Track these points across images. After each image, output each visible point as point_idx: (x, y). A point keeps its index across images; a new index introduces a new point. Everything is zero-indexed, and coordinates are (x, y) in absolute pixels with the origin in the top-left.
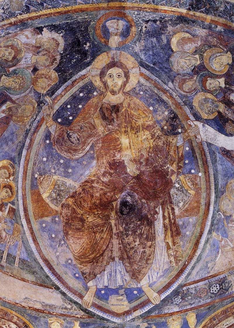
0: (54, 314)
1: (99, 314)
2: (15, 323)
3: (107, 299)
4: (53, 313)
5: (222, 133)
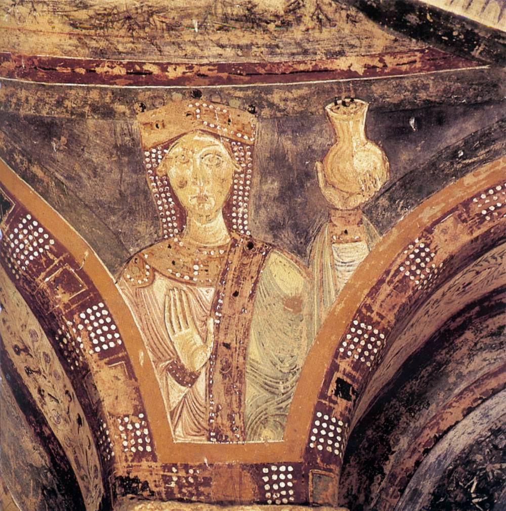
0: (172, 74)
4: (164, 67)
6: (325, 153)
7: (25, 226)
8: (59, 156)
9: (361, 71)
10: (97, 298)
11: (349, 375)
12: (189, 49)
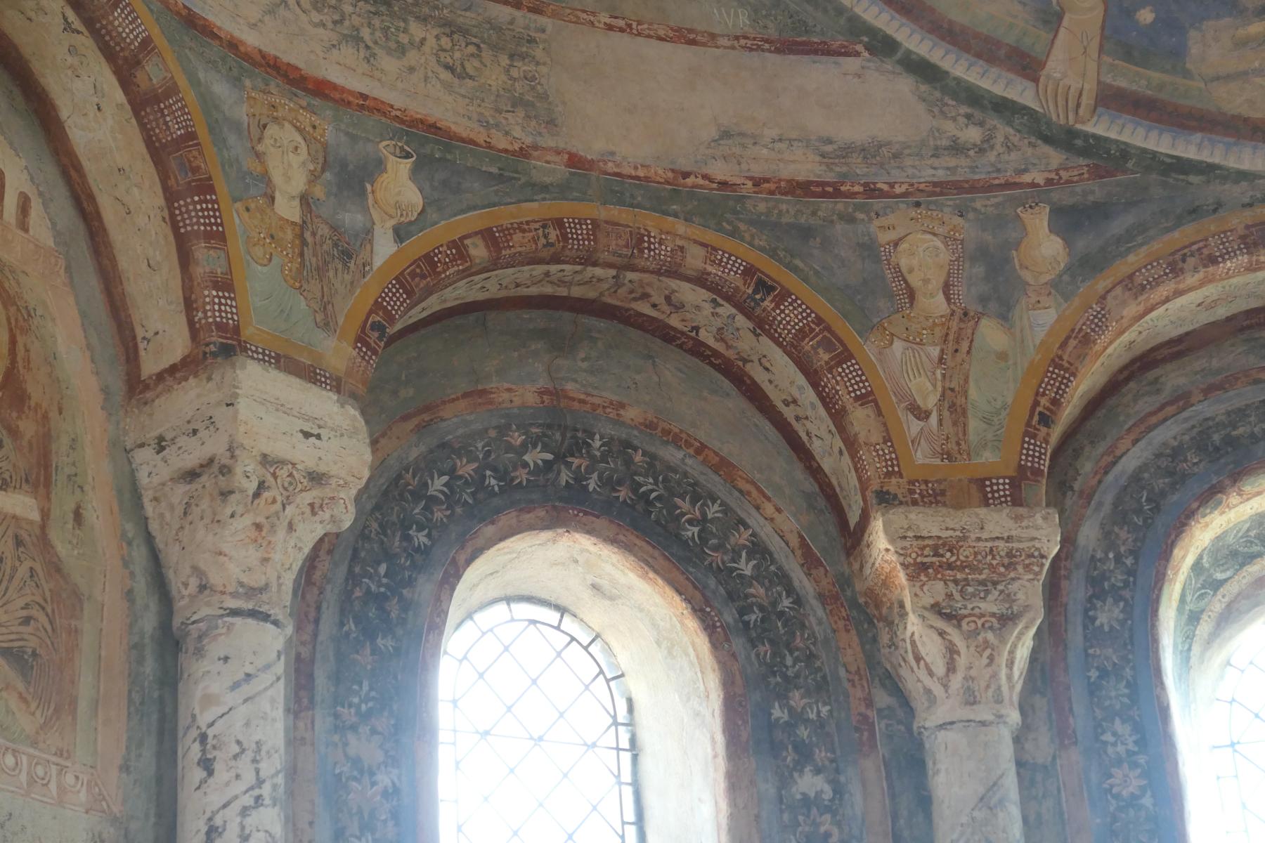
0: (898, 190)
1: (1151, 145)
2: (701, 280)
3: (1177, 54)
4: (892, 185)
6: (1017, 245)
7: (791, 304)
8: (816, 252)
9: (1042, 183)
10: (851, 357)
11: (1048, 409)
12: (910, 171)
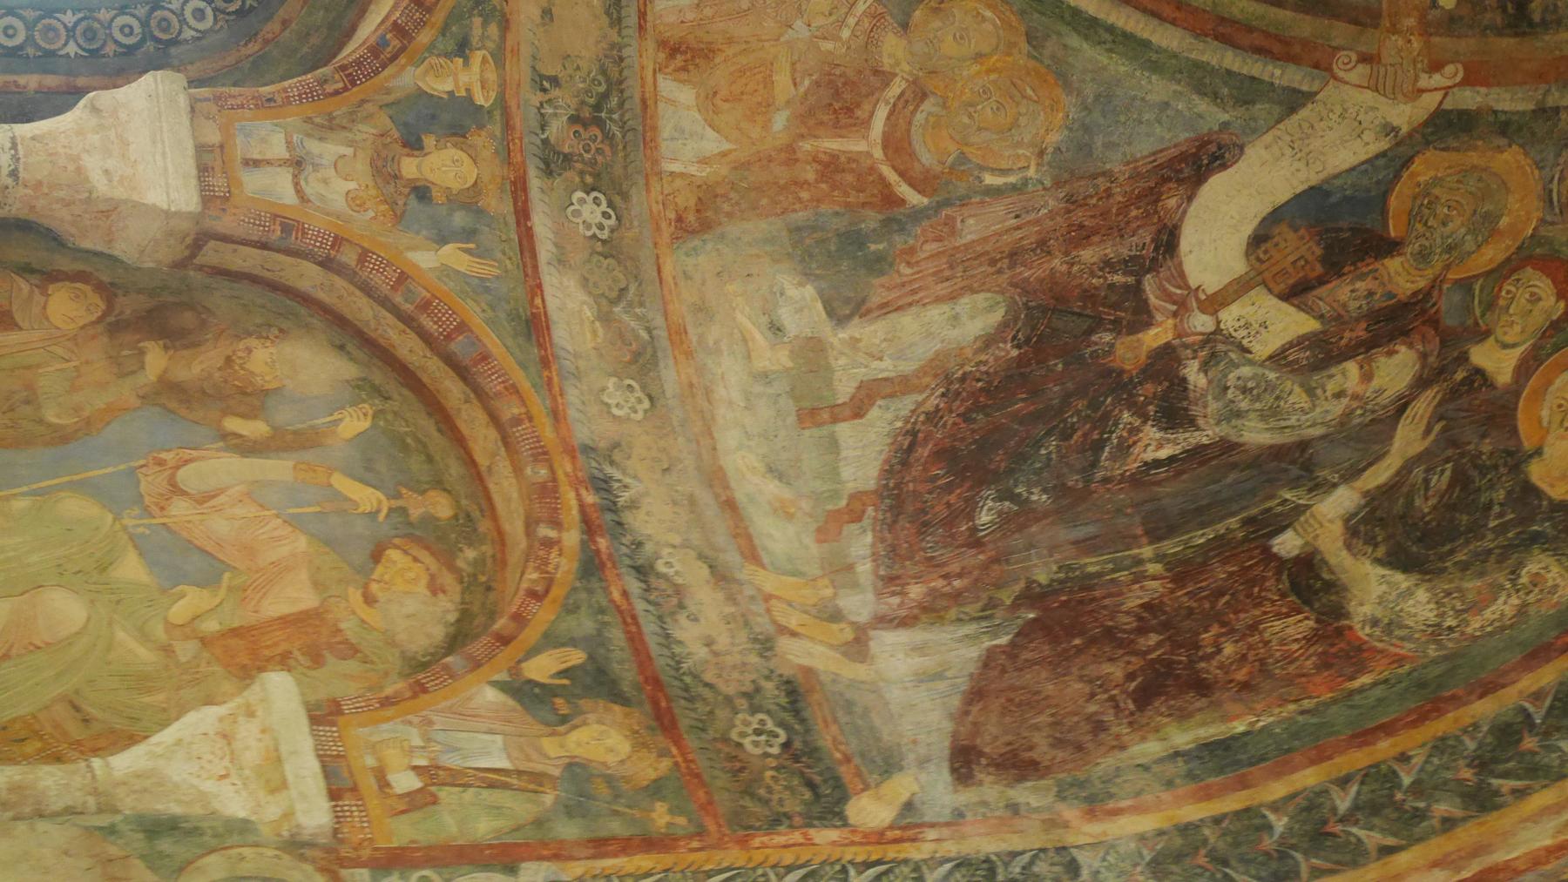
5: (1297, 197)
